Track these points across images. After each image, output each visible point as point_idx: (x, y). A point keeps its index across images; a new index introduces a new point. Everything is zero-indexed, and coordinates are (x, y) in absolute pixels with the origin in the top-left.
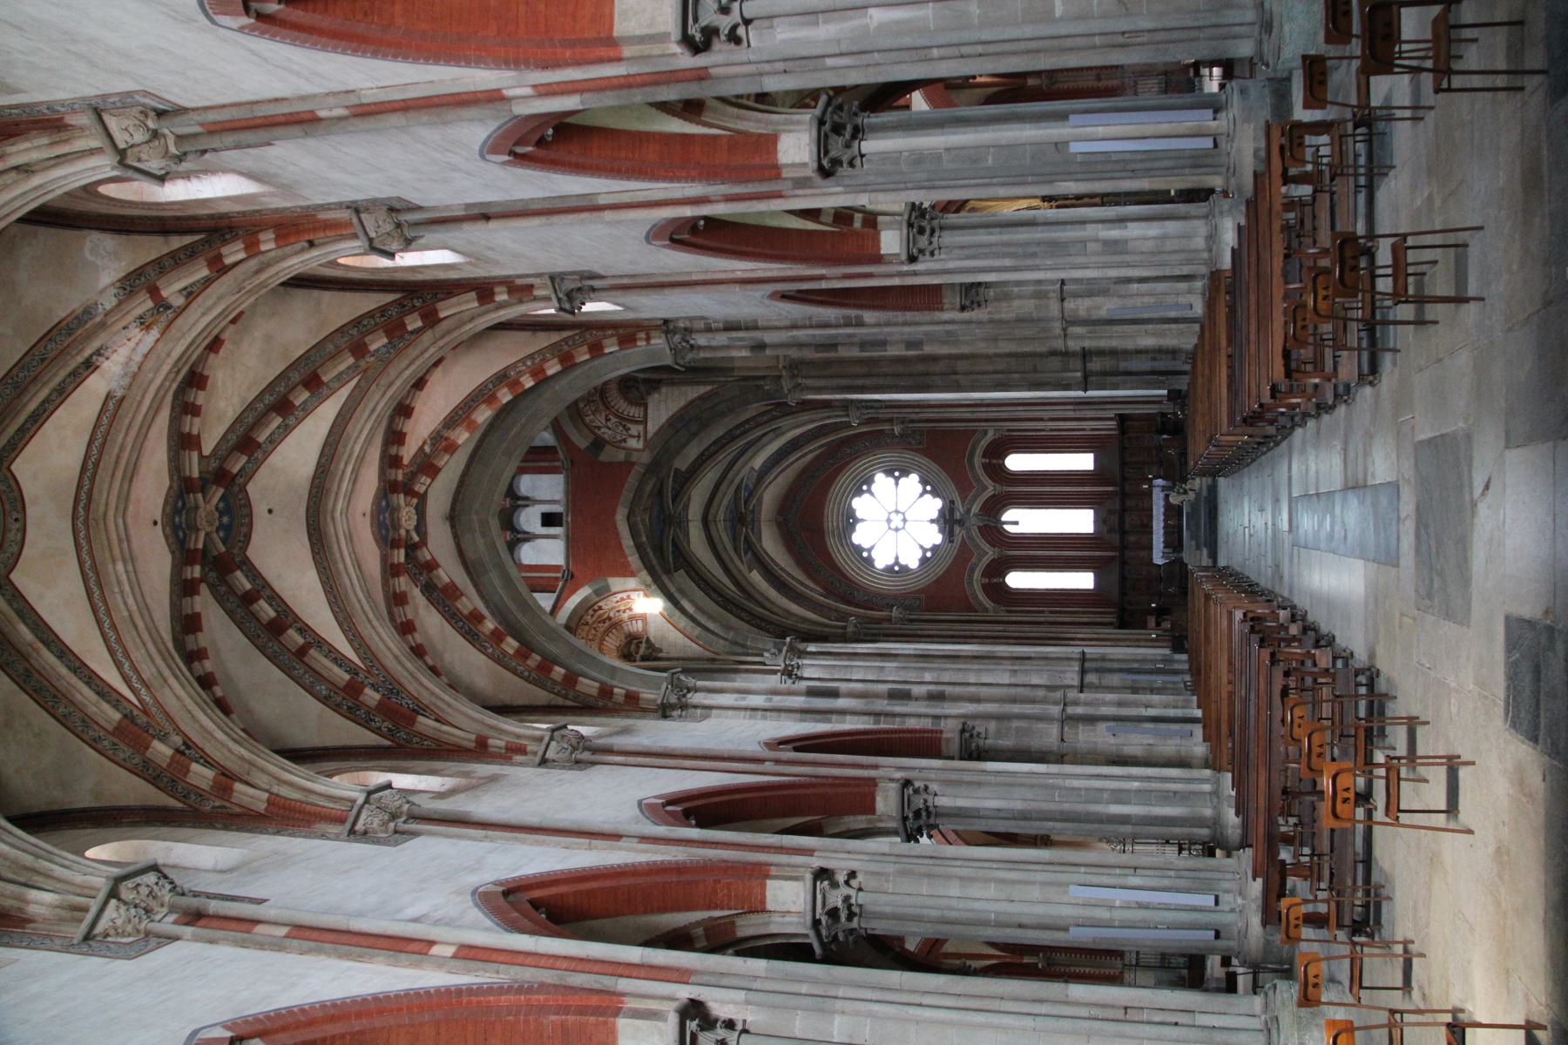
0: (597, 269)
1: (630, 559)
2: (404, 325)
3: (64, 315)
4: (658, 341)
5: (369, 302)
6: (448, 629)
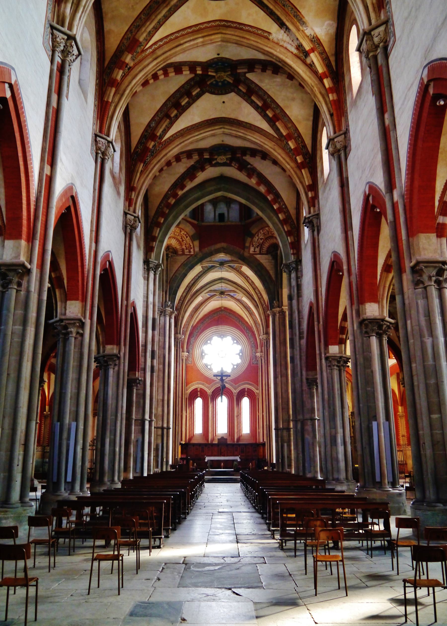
0: (322, 232)
1: (206, 249)
2: (299, 155)
3: (302, 13)
4: (293, 258)
5: (308, 141)
6: (178, 176)
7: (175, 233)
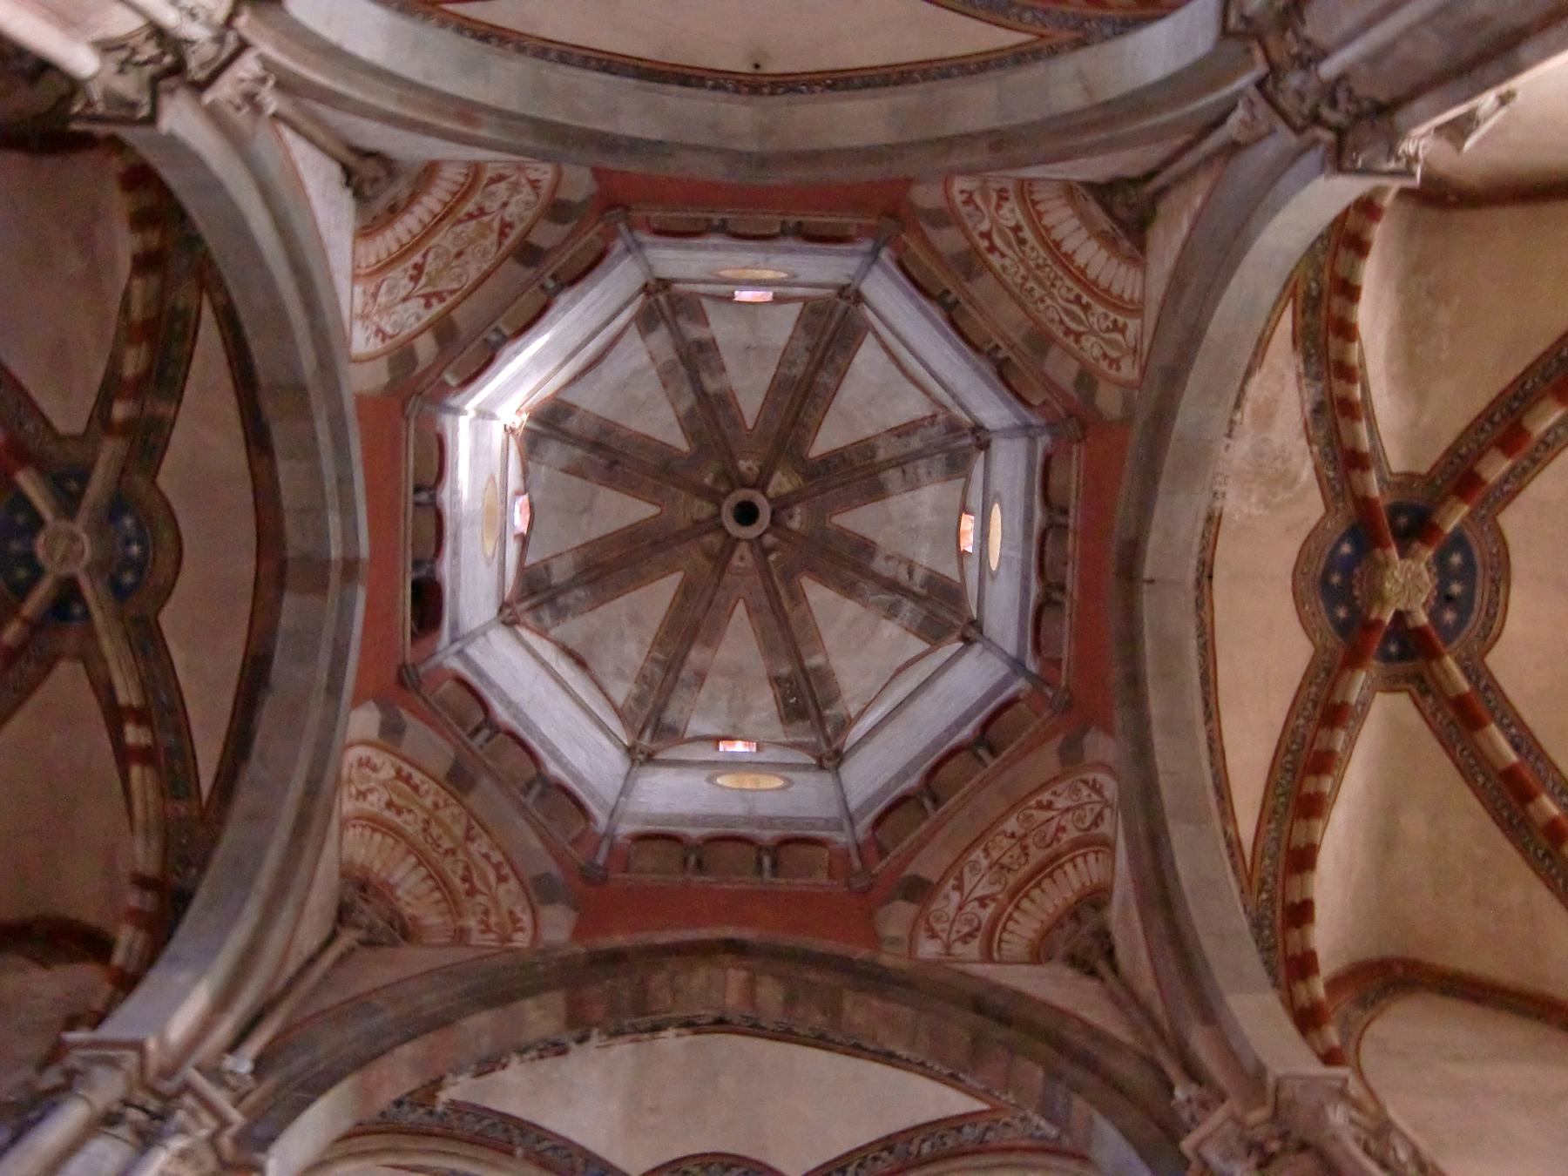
7: (435, 830)
